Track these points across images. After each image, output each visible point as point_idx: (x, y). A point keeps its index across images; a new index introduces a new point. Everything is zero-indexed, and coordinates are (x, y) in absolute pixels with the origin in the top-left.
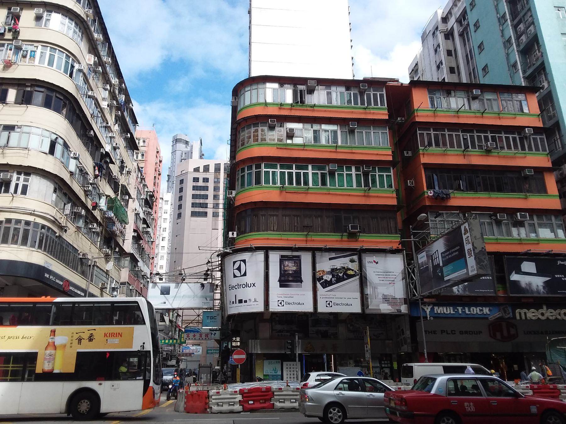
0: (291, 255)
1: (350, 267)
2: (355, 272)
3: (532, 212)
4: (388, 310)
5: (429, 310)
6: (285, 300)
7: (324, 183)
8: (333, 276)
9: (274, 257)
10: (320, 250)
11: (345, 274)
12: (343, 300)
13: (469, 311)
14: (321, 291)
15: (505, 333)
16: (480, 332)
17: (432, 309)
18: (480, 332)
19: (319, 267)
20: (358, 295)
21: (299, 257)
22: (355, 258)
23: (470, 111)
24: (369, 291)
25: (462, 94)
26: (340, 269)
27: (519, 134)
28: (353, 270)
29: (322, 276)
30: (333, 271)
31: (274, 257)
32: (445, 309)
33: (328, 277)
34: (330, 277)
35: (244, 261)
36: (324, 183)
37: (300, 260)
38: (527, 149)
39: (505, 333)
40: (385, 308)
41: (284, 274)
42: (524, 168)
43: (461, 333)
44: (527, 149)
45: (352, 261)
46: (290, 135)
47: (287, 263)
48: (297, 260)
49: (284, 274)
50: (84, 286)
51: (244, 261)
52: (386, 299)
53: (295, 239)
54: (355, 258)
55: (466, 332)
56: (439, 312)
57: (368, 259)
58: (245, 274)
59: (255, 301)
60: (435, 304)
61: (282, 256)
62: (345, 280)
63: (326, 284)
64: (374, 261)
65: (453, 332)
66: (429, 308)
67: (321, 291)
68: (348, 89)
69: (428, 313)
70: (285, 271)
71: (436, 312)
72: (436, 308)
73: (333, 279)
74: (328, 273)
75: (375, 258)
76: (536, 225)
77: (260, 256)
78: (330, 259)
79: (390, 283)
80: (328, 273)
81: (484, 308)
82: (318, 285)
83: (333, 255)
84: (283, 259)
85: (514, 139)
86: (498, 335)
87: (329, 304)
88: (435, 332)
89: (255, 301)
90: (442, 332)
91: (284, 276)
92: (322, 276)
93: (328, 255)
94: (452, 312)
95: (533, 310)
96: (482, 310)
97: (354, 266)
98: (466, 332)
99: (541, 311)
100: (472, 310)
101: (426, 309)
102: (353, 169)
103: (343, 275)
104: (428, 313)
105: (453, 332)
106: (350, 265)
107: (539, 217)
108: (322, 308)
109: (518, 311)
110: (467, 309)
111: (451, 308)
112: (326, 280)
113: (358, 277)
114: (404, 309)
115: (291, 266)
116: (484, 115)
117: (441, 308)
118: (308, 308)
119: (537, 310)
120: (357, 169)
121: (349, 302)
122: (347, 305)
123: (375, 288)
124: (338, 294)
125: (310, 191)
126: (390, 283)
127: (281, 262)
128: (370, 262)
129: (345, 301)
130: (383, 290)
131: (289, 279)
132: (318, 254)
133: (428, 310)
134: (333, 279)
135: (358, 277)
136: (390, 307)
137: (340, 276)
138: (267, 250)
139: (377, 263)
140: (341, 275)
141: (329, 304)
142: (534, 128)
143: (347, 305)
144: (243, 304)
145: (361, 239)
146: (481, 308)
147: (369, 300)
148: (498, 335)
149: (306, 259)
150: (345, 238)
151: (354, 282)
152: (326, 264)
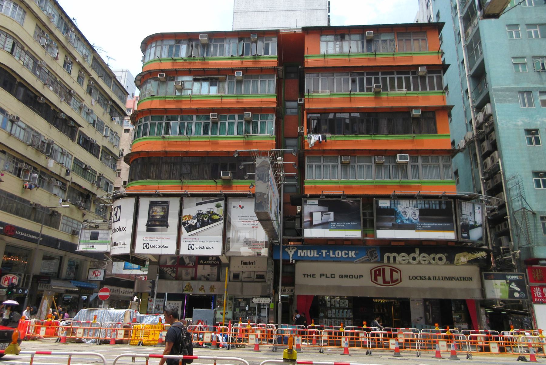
0: (160, 202)
1: (215, 212)
2: (220, 216)
3: (414, 154)
4: (248, 252)
5: (293, 253)
6: (196, 244)
7: (206, 132)
8: (198, 221)
9: (144, 204)
10: (186, 195)
11: (210, 218)
12: (206, 243)
13: (334, 254)
14: (185, 233)
15: (388, 278)
16: (361, 276)
17: (296, 252)
18: (361, 276)
19: (185, 212)
20: (220, 238)
21: (167, 203)
22: (222, 203)
23: (363, 54)
24: (231, 235)
25: (357, 37)
26: (205, 214)
27: (414, 73)
28: (217, 215)
29: (187, 221)
30: (198, 216)
31: (144, 204)
32: (309, 251)
33: (193, 222)
34: (195, 221)
35: (120, 207)
36: (206, 132)
37: (168, 206)
38: (420, 88)
39: (388, 278)
40: (246, 251)
41: (152, 219)
42: (411, 108)
43: (341, 277)
44: (420, 88)
45: (218, 206)
46: (181, 89)
47: (155, 208)
48: (165, 206)
49: (152, 219)
50: (38, 231)
51: (120, 207)
52: (247, 242)
53: (171, 186)
54: (222, 203)
55: (346, 276)
56: (302, 255)
57: (233, 203)
58: (119, 220)
59: (124, 244)
60: (298, 248)
61: (152, 202)
62: (208, 224)
63: (191, 228)
64: (240, 206)
65: (333, 276)
66: (293, 251)
67: (185, 233)
68: (240, 40)
69: (291, 256)
70: (153, 216)
71: (299, 255)
72: (300, 251)
73: (198, 224)
74: (194, 218)
75: (241, 202)
76: (420, 166)
77: (132, 201)
78: (197, 204)
79: (253, 227)
80: (194, 218)
81: (350, 252)
82: (183, 229)
83: (200, 200)
84: (152, 204)
85: (408, 80)
86: (380, 279)
87: (146, 246)
88: (313, 276)
89: (124, 244)
90: (321, 275)
91: (152, 221)
92: (187, 221)
93: (195, 200)
94: (316, 255)
95: (403, 254)
96: (348, 254)
97: (220, 211)
98: (346, 276)
99: (412, 255)
100: (336, 253)
101: (289, 252)
102: (236, 117)
103: (208, 220)
104: (291, 256)
105: (332, 276)
106: (216, 210)
107: (425, 159)
108: (184, 251)
109: (386, 255)
110: (331, 252)
111: (316, 251)
112: (191, 225)
113: (222, 221)
114: (264, 252)
115: (159, 212)
116: (377, 57)
117: (305, 251)
118: (171, 250)
119: (409, 255)
120: (241, 117)
121: (211, 245)
122: (209, 248)
123: (237, 232)
124: (200, 237)
125: (191, 140)
126: (253, 227)
127: (151, 207)
128: (234, 207)
129: (206, 244)
130: (245, 234)
131: (156, 223)
132: (186, 200)
133: (291, 253)
134: (198, 224)
135: (222, 221)
136: (250, 250)
137: (205, 220)
138: (137, 197)
139: (242, 208)
140: (206, 219)
141: (191, 247)
142: (428, 66)
143: (209, 248)
144: (116, 246)
145: (234, 185)
146: (347, 252)
147: (231, 243)
148: (380, 279)
149: (174, 204)
150: (220, 185)
151: (219, 226)
152: (192, 210)
